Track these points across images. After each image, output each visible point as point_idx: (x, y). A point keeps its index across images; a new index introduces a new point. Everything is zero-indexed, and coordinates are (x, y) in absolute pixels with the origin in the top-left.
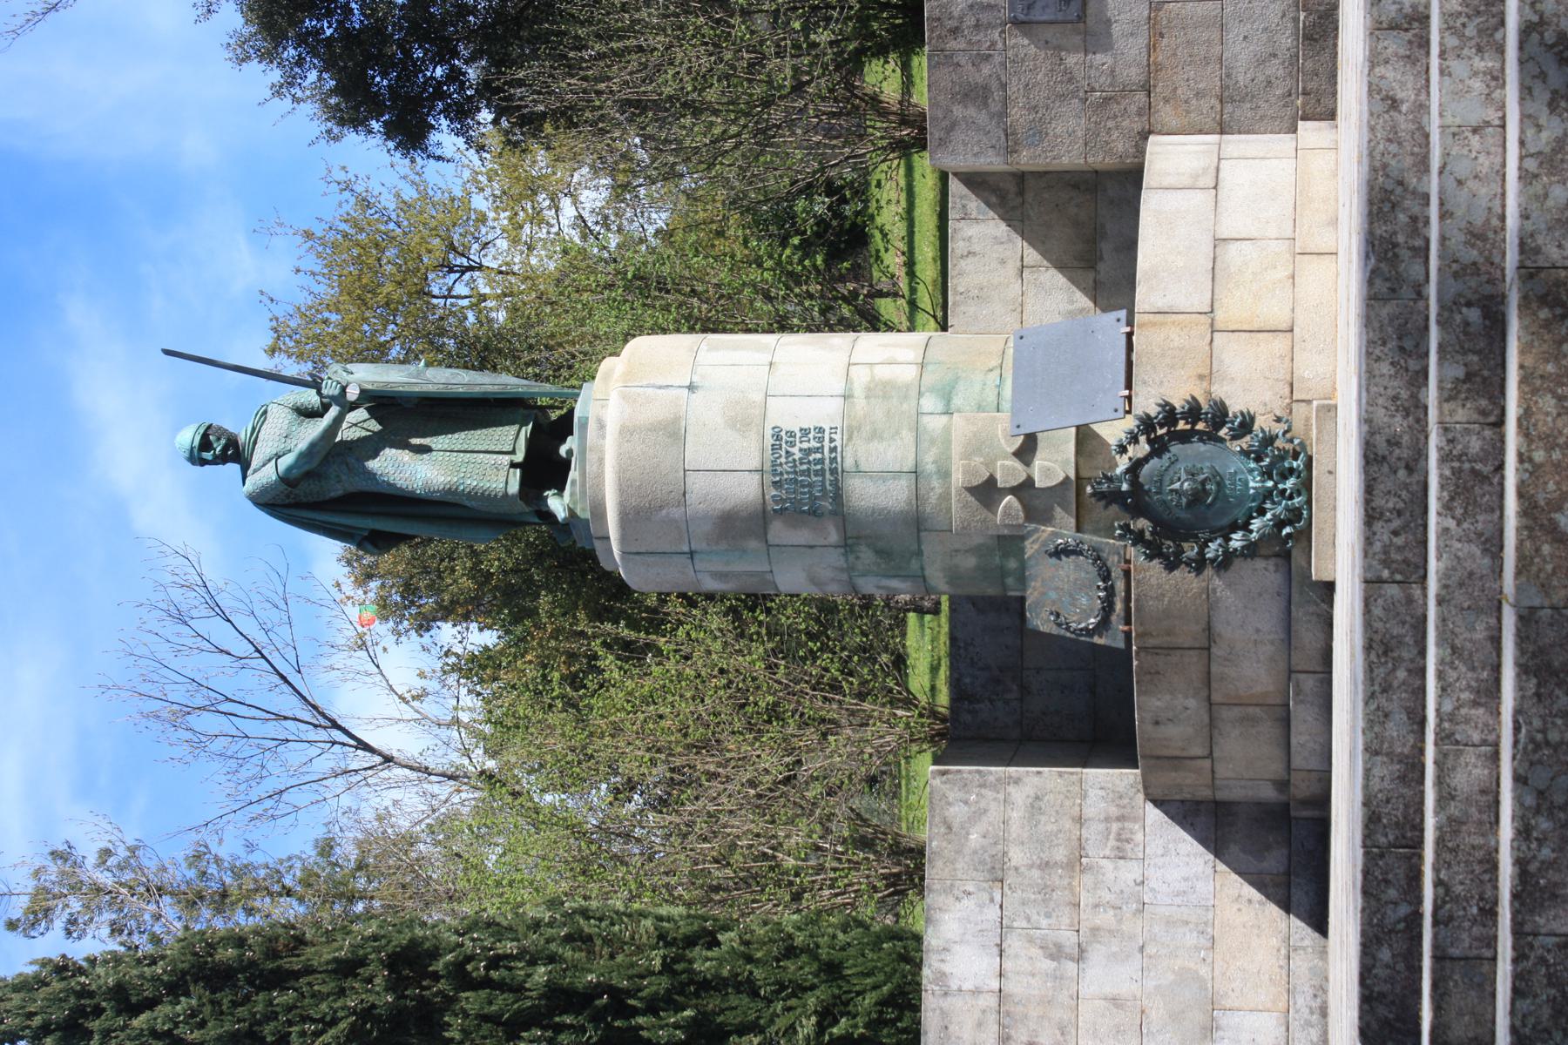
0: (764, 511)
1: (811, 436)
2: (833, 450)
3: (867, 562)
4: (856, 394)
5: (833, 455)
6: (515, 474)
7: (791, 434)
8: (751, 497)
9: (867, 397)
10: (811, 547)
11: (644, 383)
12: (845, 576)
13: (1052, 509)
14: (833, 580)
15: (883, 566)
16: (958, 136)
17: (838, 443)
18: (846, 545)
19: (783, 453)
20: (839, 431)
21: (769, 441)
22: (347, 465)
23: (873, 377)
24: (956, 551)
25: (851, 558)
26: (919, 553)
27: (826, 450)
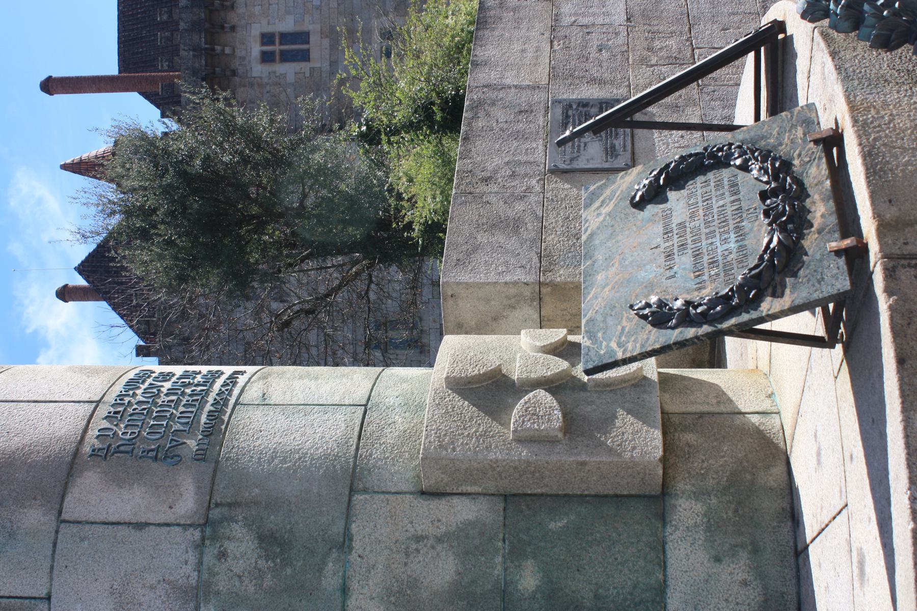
0: (76, 453)
10: (140, 526)
13: (615, 417)
16: (481, 258)
18: (207, 522)
24: (419, 539)
26: (345, 543)
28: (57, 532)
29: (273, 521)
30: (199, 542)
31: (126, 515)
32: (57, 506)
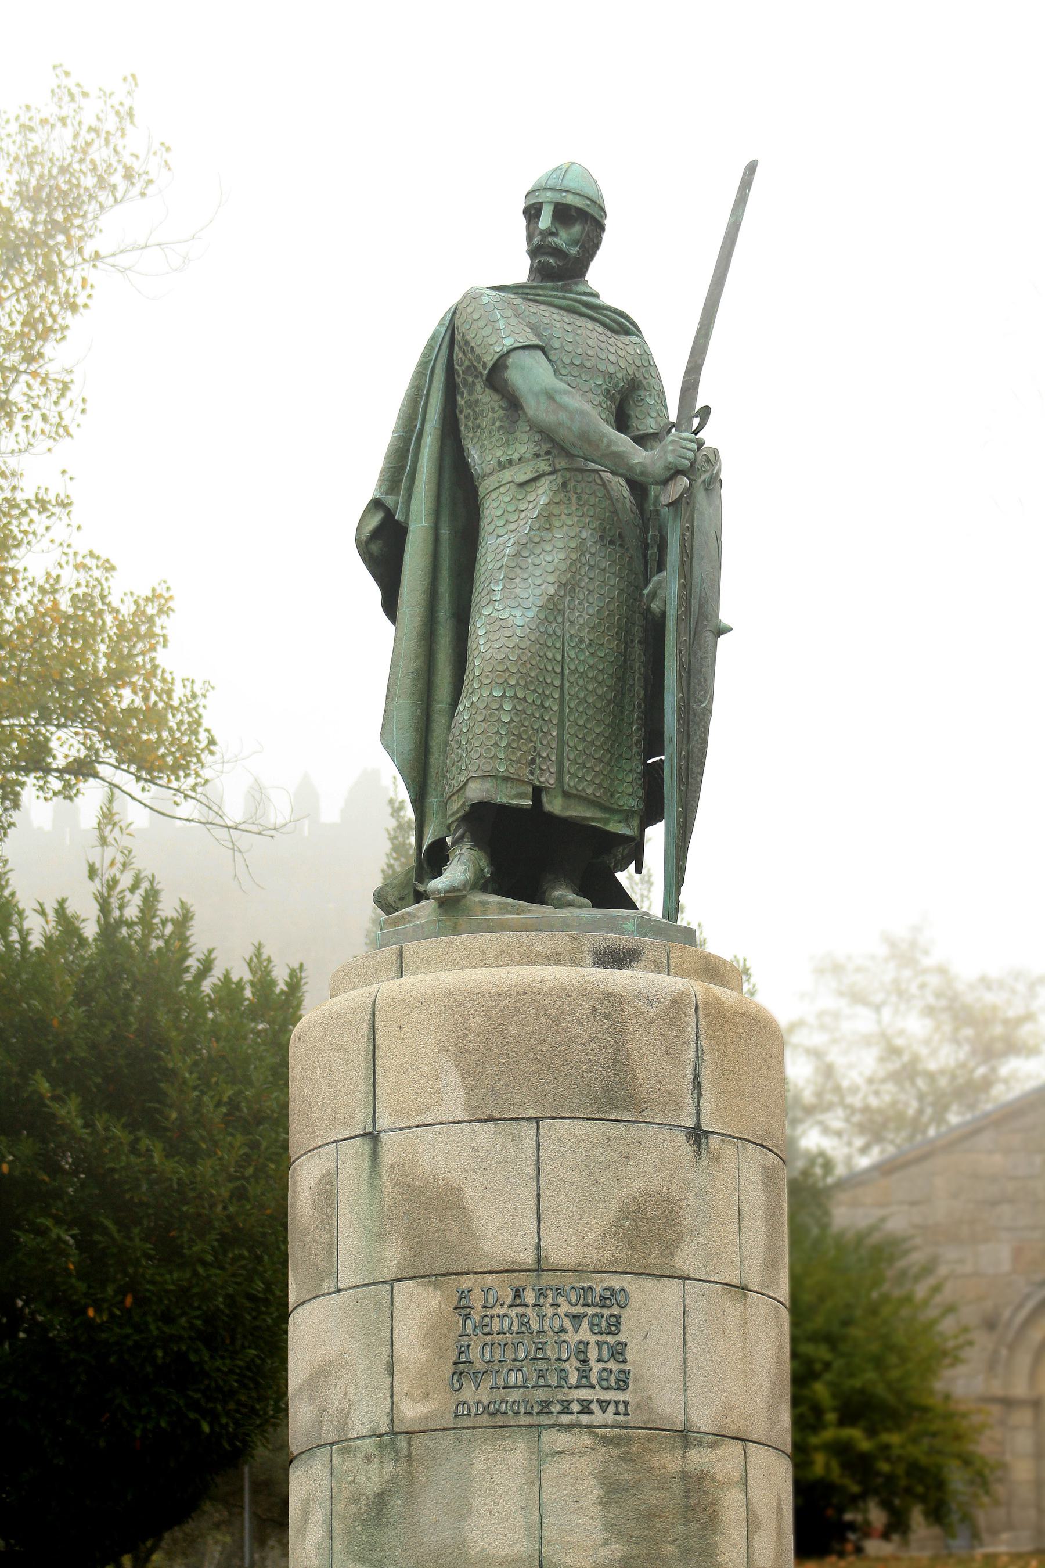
1: (612, 1365)
2: (586, 1408)
3: (361, 1478)
4: (692, 1453)
5: (575, 1407)
6: (520, 796)
7: (615, 1325)
8: (488, 1247)
9: (685, 1475)
11: (704, 1042)
12: (331, 1437)
14: (323, 1410)
15: (353, 1509)
17: (598, 1417)
19: (578, 1310)
20: (621, 1418)
21: (600, 1283)
22: (534, 480)
23: (725, 1486)
25: (368, 1446)
27: (584, 1394)
28: (383, 1282)
29: (396, 1503)
30: (378, 1432)
31: (400, 1350)
32: (405, 1275)
